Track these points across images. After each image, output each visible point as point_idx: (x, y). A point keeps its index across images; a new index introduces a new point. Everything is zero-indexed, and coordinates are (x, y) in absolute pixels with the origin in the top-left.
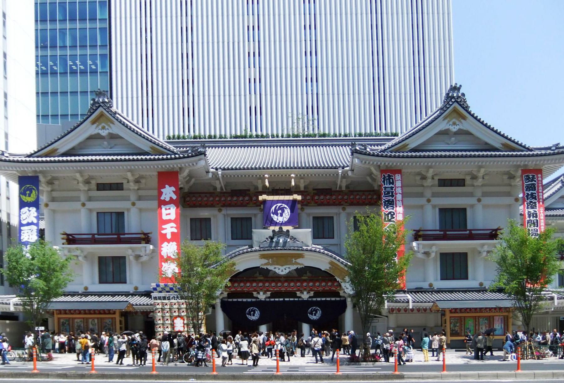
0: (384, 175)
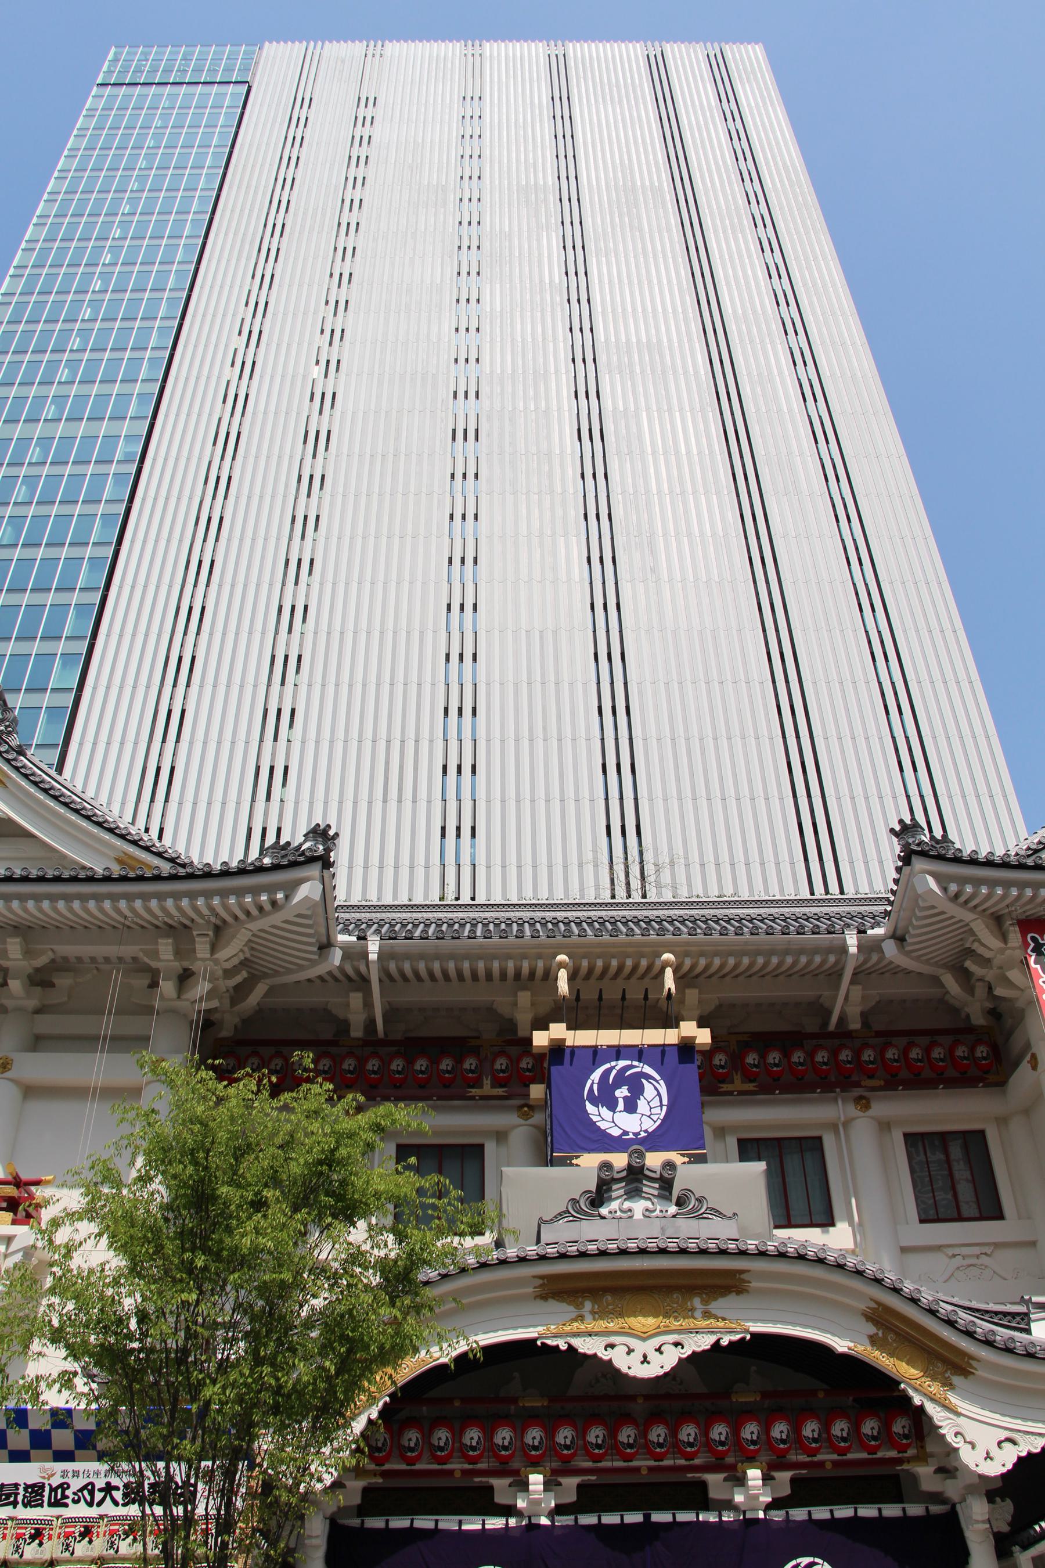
0: (1033, 939)
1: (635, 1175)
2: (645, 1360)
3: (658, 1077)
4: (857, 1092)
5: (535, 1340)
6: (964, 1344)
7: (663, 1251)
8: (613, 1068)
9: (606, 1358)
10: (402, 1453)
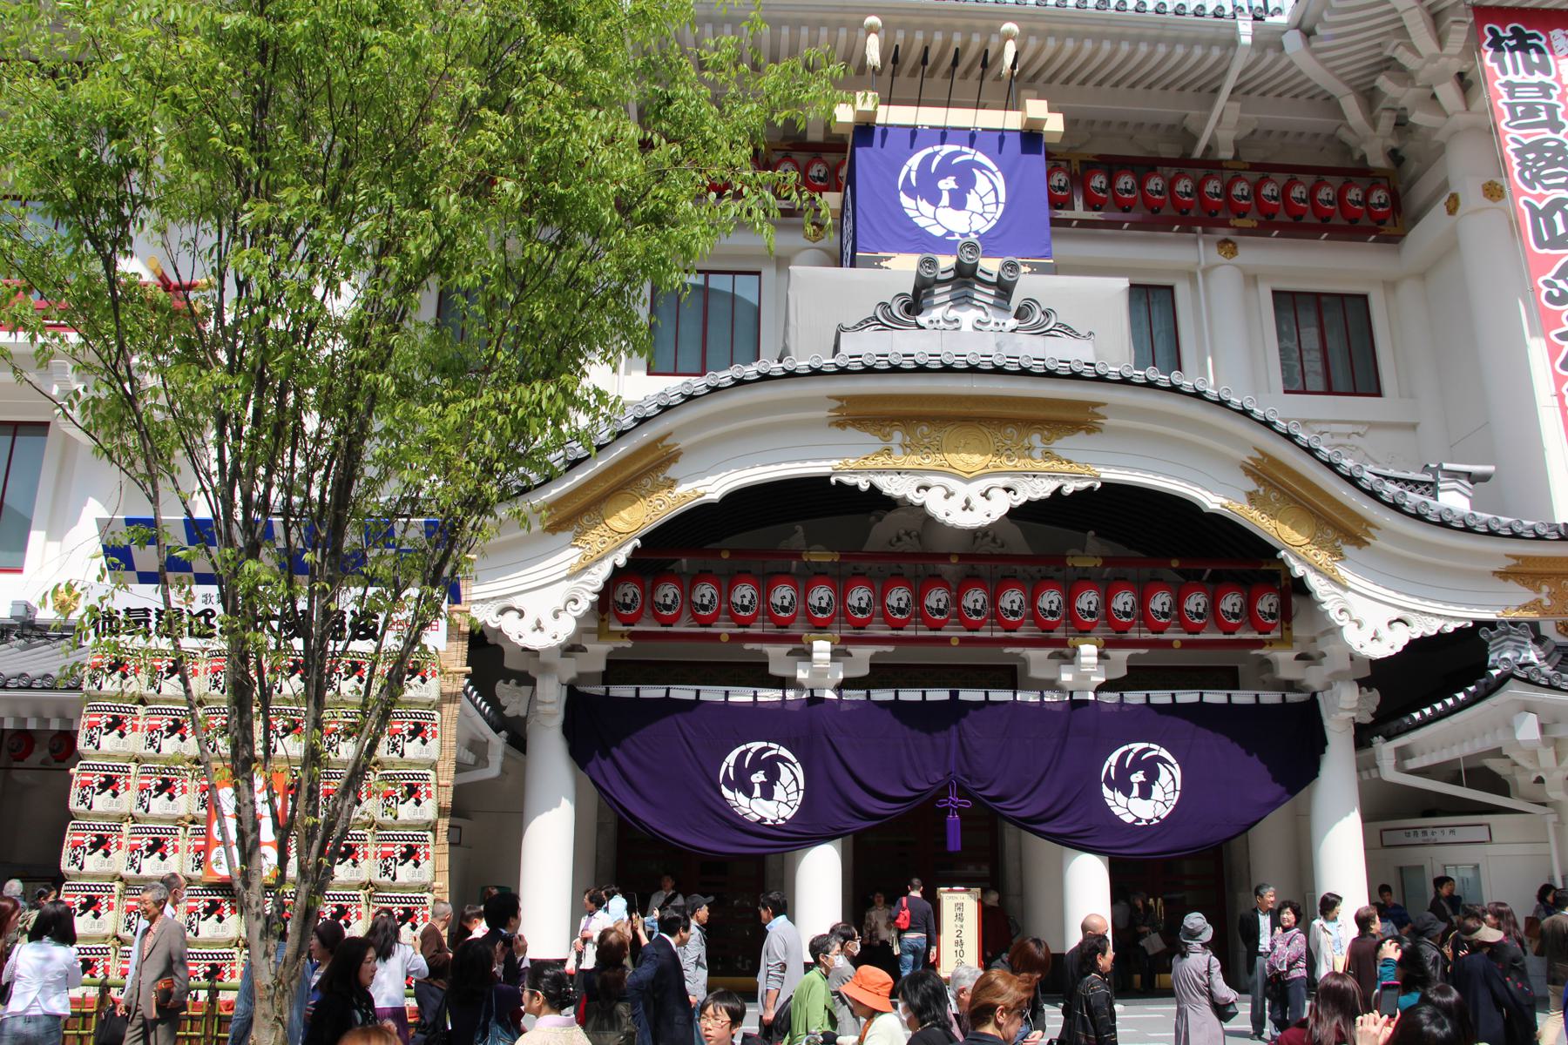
1: (965, 276)
2: (967, 506)
3: (994, 168)
4: (1223, 233)
5: (827, 478)
6: (1366, 507)
7: (998, 371)
8: (936, 153)
9: (918, 502)
10: (656, 611)
